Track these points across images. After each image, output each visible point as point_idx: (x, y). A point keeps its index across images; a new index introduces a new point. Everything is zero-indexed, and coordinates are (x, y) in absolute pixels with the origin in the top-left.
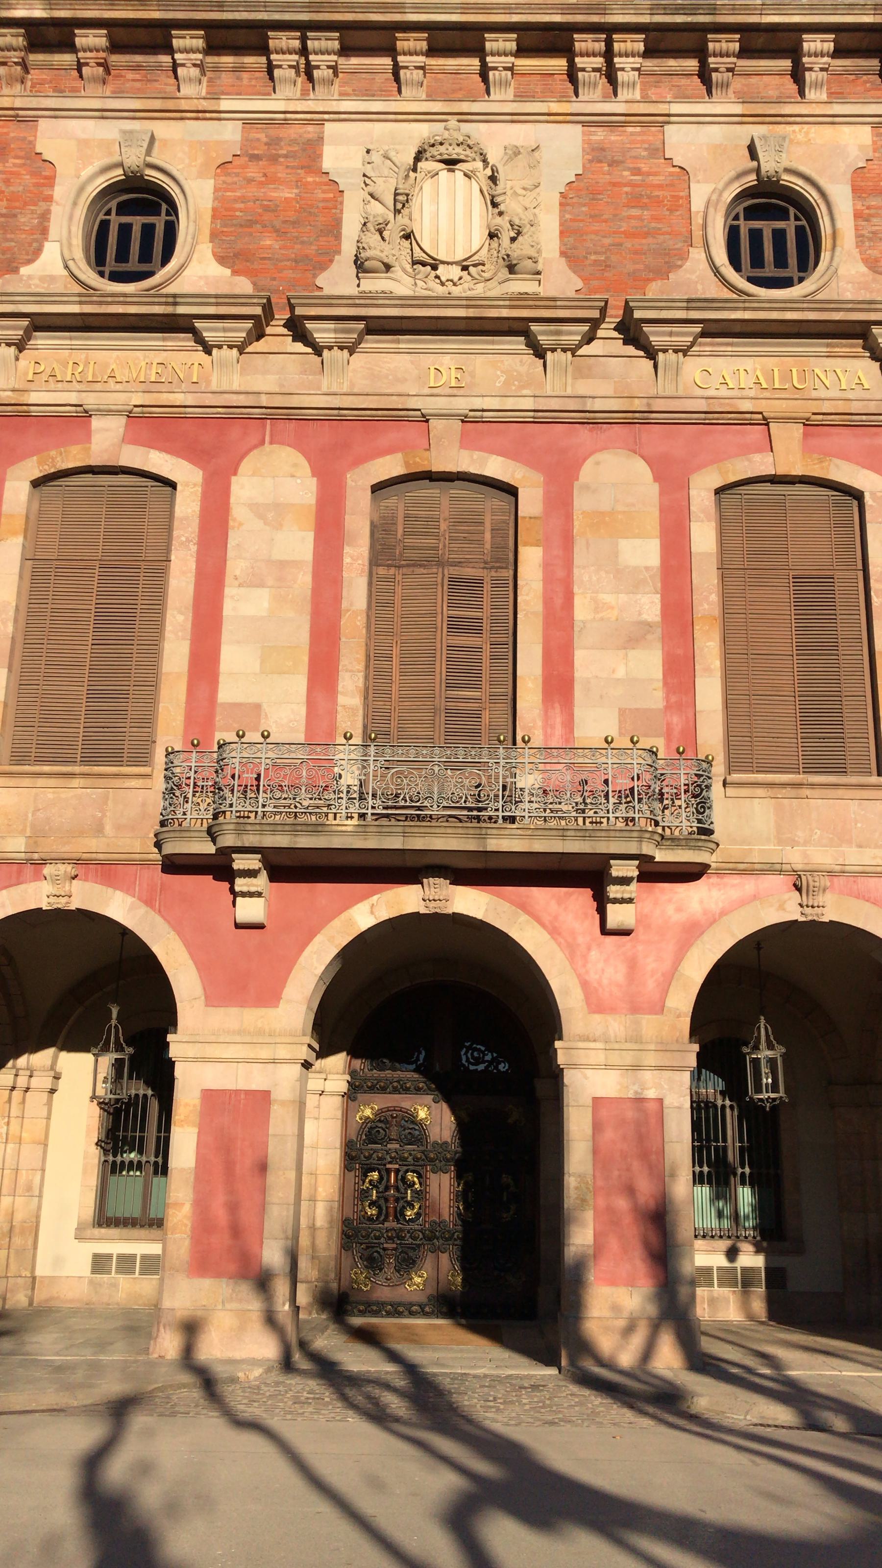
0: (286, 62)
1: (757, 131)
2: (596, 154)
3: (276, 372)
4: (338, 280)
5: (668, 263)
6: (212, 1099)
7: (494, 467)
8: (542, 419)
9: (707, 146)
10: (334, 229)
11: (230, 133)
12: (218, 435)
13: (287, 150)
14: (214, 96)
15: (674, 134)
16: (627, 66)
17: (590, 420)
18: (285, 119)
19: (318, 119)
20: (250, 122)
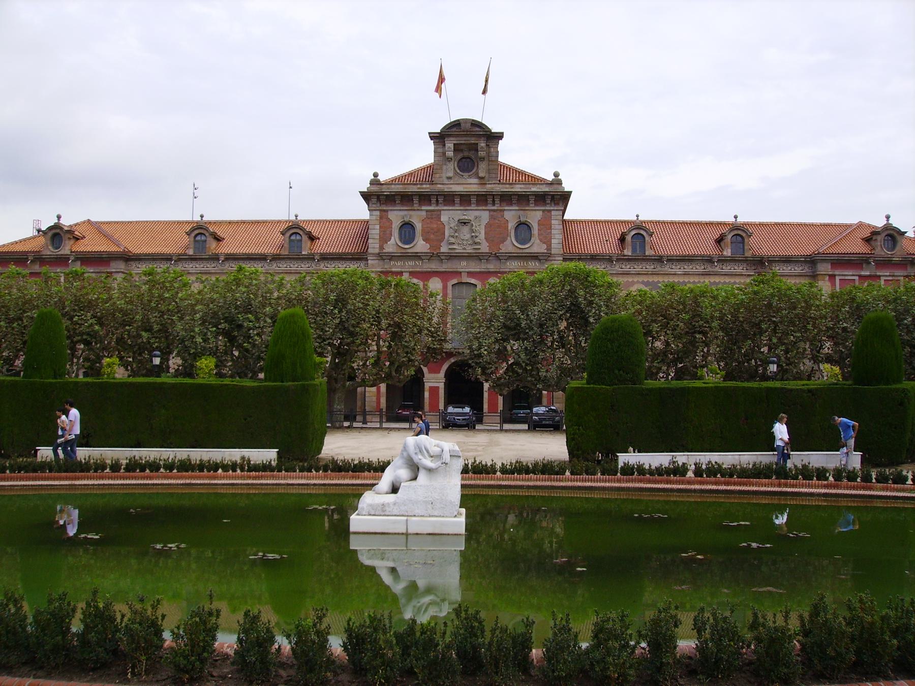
0: (434, 200)
1: (522, 212)
2: (491, 217)
3: (434, 266)
4: (444, 249)
5: (503, 240)
6: (431, 388)
7: (473, 281)
8: (480, 272)
9: (511, 215)
10: (444, 234)
11: (424, 213)
12: (426, 276)
13: (435, 216)
14: (420, 205)
15: (506, 213)
16: (497, 201)
17: (489, 272)
18: (433, 211)
19: (440, 211)
20: (427, 211)
